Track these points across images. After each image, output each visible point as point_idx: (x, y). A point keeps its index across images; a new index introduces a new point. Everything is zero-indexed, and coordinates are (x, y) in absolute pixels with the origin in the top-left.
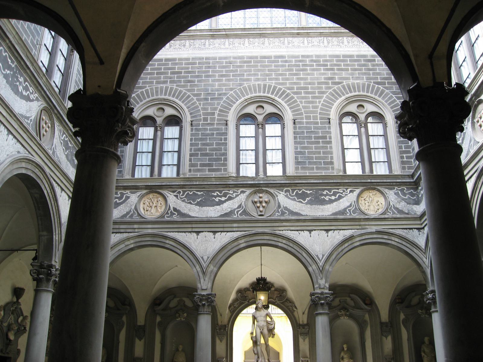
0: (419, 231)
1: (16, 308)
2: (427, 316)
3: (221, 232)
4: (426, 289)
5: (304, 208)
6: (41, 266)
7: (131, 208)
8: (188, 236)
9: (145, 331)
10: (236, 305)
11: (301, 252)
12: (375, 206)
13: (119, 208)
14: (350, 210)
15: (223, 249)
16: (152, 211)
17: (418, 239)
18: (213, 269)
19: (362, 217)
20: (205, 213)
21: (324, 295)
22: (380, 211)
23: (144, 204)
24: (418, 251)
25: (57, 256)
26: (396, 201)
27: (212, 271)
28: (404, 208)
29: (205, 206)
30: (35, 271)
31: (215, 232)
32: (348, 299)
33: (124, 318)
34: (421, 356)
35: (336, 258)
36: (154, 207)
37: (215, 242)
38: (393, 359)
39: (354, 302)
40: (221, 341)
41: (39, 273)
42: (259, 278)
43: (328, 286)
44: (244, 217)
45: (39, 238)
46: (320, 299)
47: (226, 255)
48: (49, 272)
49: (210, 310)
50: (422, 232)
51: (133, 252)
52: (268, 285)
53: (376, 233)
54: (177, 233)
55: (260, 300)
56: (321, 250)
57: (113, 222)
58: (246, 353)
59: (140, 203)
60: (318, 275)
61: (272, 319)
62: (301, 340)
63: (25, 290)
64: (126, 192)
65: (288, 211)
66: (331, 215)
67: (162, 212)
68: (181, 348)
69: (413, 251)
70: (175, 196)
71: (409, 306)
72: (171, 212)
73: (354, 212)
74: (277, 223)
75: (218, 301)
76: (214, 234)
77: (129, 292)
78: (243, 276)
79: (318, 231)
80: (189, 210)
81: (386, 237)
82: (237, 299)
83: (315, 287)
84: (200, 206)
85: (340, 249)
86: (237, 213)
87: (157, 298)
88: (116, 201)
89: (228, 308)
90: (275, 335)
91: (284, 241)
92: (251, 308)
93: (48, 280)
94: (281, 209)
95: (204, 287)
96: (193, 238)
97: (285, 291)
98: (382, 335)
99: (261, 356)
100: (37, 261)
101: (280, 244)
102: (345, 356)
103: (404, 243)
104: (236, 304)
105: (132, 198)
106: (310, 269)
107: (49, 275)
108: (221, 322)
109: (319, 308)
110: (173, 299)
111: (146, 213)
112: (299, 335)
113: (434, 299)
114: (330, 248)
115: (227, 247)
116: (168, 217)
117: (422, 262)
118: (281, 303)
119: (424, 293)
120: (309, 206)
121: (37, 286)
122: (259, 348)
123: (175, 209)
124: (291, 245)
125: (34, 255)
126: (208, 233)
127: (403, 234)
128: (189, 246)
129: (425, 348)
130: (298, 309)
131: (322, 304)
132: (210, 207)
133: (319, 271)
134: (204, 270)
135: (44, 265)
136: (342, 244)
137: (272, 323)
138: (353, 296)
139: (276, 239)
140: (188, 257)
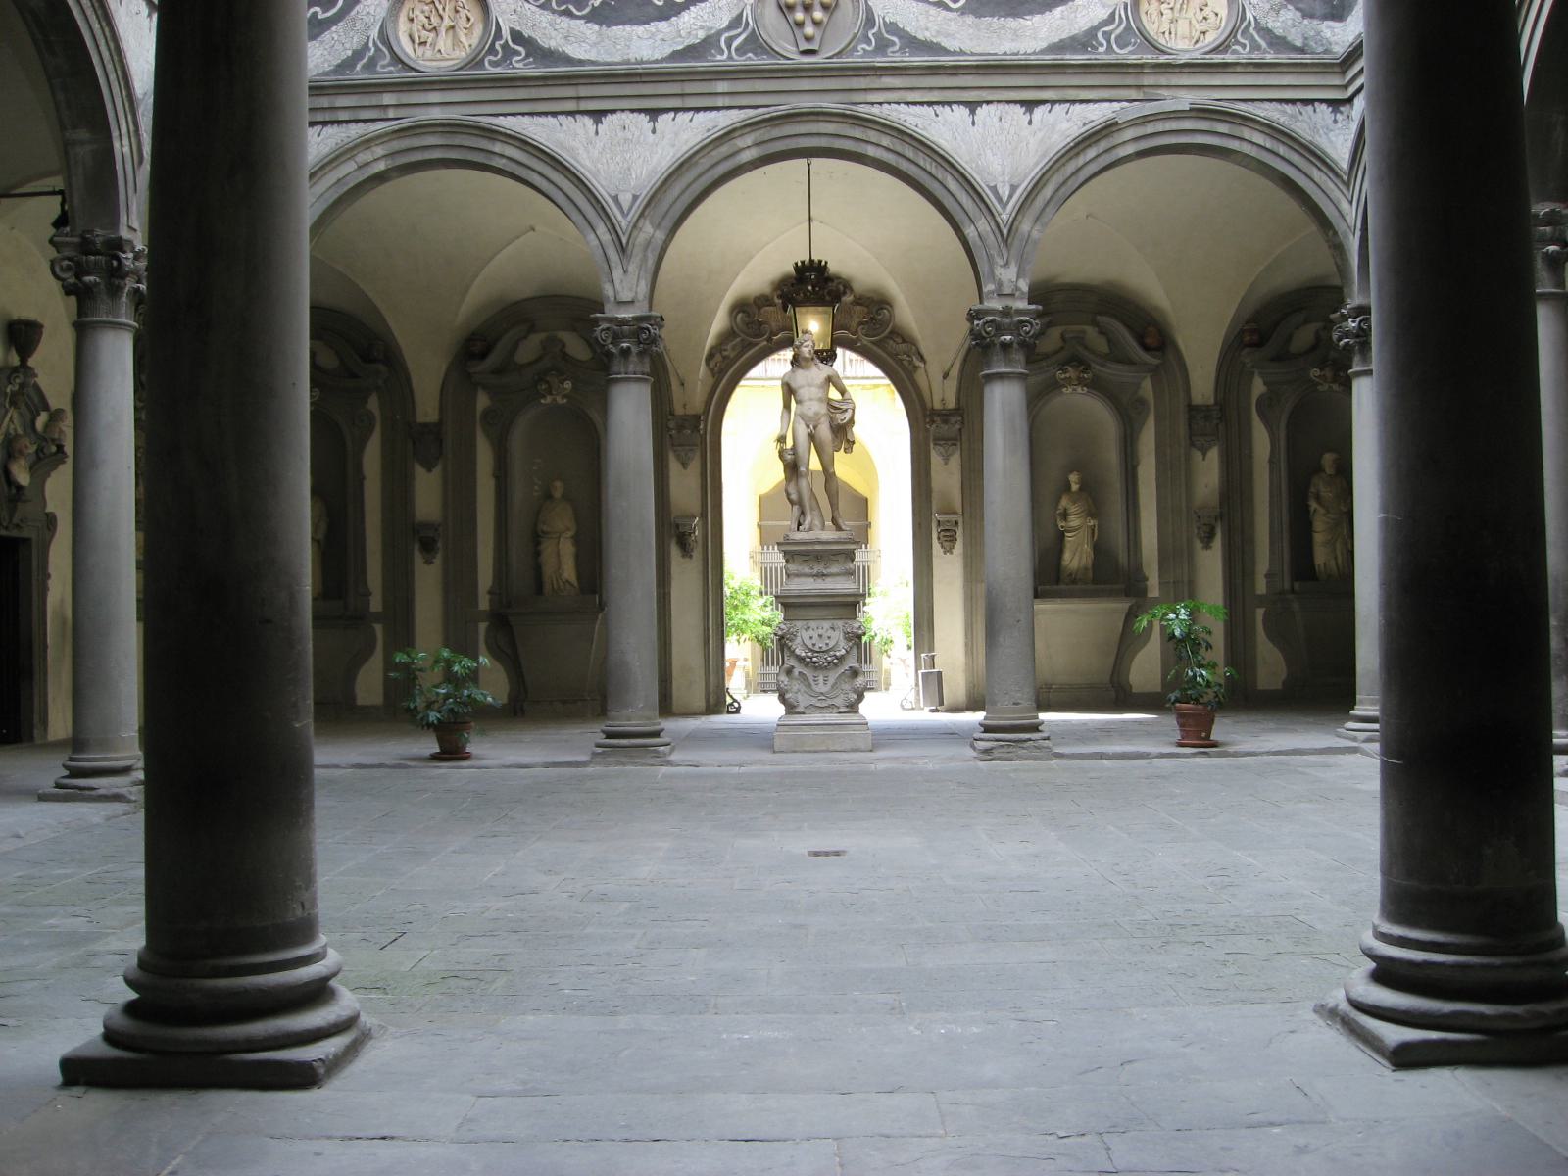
0: (1335, 111)
1: (22, 386)
2: (1335, 387)
3: (677, 110)
4: (1341, 302)
5: (953, 28)
6: (86, 247)
7: (369, 38)
8: (565, 128)
9: (441, 441)
10: (729, 352)
11: (940, 177)
12: (1194, 22)
13: (327, 36)
14: (1111, 33)
15: (684, 168)
16: (441, 45)
17: (1329, 139)
18: (653, 235)
19: (1149, 58)
20: (619, 47)
21: (1012, 317)
22: (1212, 39)
23: (412, 20)
24: (1324, 178)
25: (134, 208)
26: (1268, 6)
27: (648, 243)
28: (1293, 30)
29: (617, 24)
30: (66, 262)
31: (654, 113)
32: (1091, 332)
33: (373, 404)
34: (1308, 506)
35: (1056, 199)
36: (447, 30)
37: (656, 145)
38: (1221, 517)
39: (1109, 341)
40: (685, 465)
41: (80, 271)
42: (803, 262)
43: (1025, 289)
44: (752, 60)
45: (66, 153)
46: (1000, 329)
47: (694, 186)
48: (115, 263)
49: (647, 370)
50: (1345, 113)
51: (386, 188)
52: (832, 286)
53: (1193, 114)
54: (527, 119)
55: (805, 332)
56: (1008, 170)
57: (310, 88)
58: (764, 501)
60: (994, 252)
61: (846, 396)
62: (936, 459)
63: (41, 326)
65: (900, 38)
66: (1043, 52)
67: (473, 47)
68: (558, 489)
69: (1306, 175)
71: (1283, 356)
72: (505, 46)
73: (1122, 42)
74: (862, 79)
75: (670, 339)
76: (653, 119)
77: (384, 320)
78: (751, 258)
79: (1000, 106)
80: (566, 37)
81: (1223, 128)
82: (734, 332)
83: (985, 290)
84: (600, 25)
85: (1071, 167)
86: (729, 47)
87: (473, 334)
88: (315, 13)
89: (703, 362)
90: (853, 442)
91: (886, 141)
92: (779, 359)
93: (114, 292)
94: (874, 31)
95: (626, 296)
96: (581, 132)
97: (891, 306)
98: (1192, 444)
99: (812, 509)
100: (68, 229)
101: (871, 151)
102: (1073, 509)
103: (1282, 150)
104: (729, 347)
106: (970, 232)
107: (115, 274)
108: (685, 405)
109: (995, 358)
110: (525, 338)
111: (420, 51)
112: (932, 445)
113: (1363, 334)
114: (1037, 164)
115: (696, 163)
116: (494, 64)
117: (1337, 213)
118: (872, 342)
119: (1332, 316)
120: (970, 19)
121: (81, 312)
122: (803, 483)
123: (517, 37)
124: (909, 152)
125: (56, 212)
126: (631, 115)
127: (1282, 120)
128: (573, 161)
129: (1322, 487)
130: (928, 364)
131: (1005, 346)
132: (635, 27)
133: (999, 239)
134: (624, 241)
135: (94, 243)
136: (1076, 150)
137: (844, 407)
138: (1104, 319)
139: (858, 133)
140: (568, 197)
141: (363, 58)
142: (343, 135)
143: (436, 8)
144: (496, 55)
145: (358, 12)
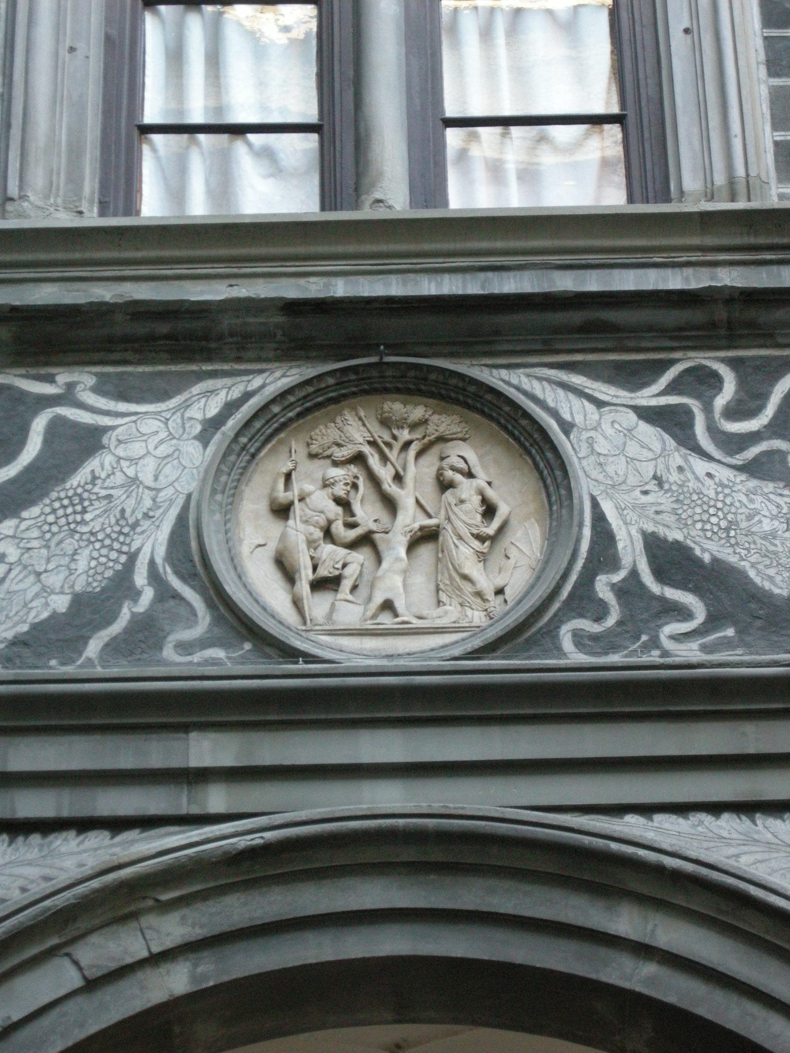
7: (132, 558)
23: (282, 511)
36: (412, 546)
54: (728, 824)
59: (234, 495)
64: (50, 379)
67: (511, 594)
70: (648, 415)
105: (137, 449)
141: (109, 621)
142: (32, 872)
143: (374, 480)
144: (598, 619)
145: (94, 478)
